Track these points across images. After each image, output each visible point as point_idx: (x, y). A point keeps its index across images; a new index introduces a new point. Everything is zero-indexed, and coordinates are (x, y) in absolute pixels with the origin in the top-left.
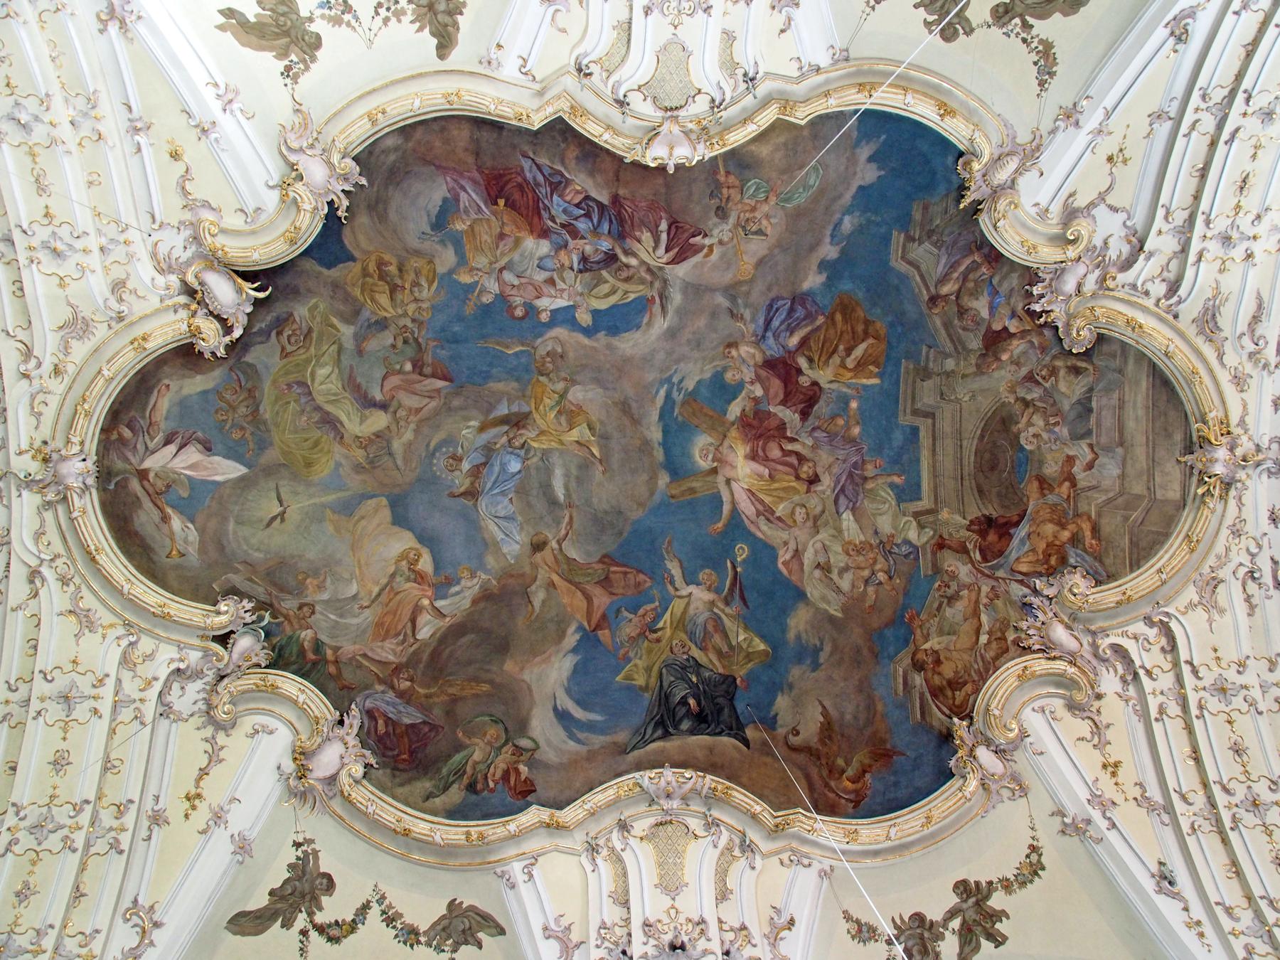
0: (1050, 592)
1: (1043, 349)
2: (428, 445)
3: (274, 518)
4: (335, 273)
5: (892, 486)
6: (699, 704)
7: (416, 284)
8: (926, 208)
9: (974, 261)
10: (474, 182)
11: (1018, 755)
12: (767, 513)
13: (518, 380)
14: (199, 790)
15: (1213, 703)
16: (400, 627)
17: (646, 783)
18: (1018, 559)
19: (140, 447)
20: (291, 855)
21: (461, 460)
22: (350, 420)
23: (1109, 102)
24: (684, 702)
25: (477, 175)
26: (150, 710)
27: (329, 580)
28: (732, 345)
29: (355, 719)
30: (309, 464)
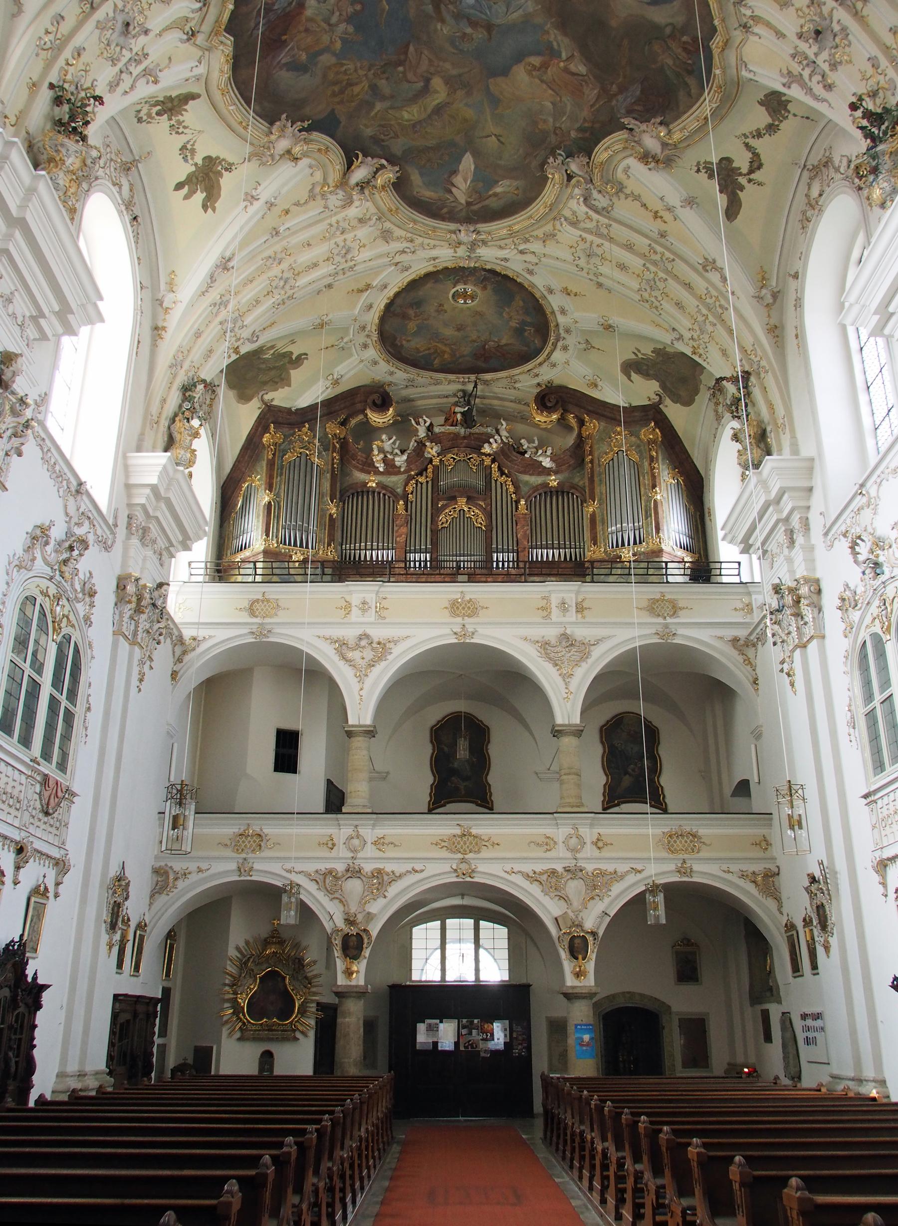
3: (499, 140)
4: (343, 119)
19: (453, 204)
20: (703, 176)
21: (465, 34)
30: (465, 120)
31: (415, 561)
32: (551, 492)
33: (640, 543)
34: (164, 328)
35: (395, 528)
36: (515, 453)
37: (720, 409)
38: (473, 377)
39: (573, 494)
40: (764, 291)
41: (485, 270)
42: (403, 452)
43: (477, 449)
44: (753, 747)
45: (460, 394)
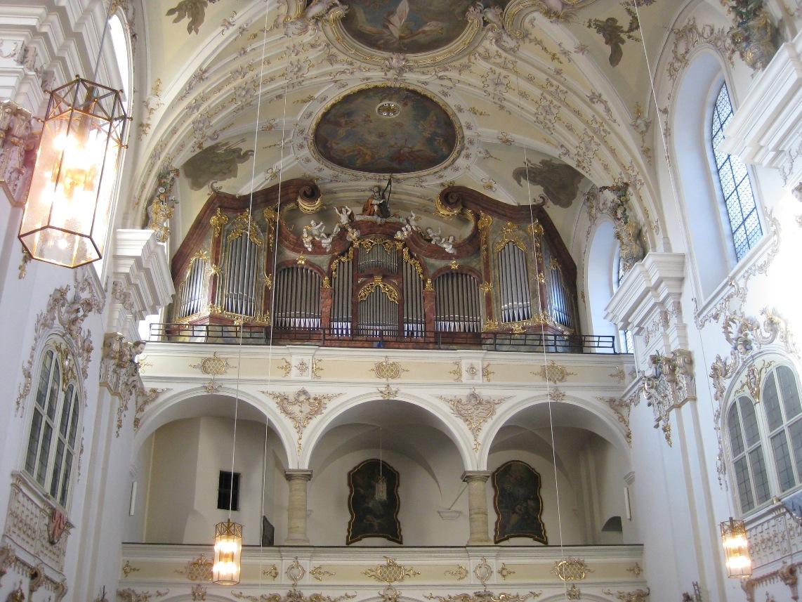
20: (593, 31)
26: (510, 57)
31: (337, 329)
32: (452, 274)
33: (528, 318)
34: (148, 125)
35: (322, 300)
36: (423, 240)
37: (594, 211)
38: (387, 176)
39: (470, 276)
40: (639, 121)
41: (408, 90)
42: (328, 235)
43: (391, 236)
44: (625, 489)
45: (376, 189)
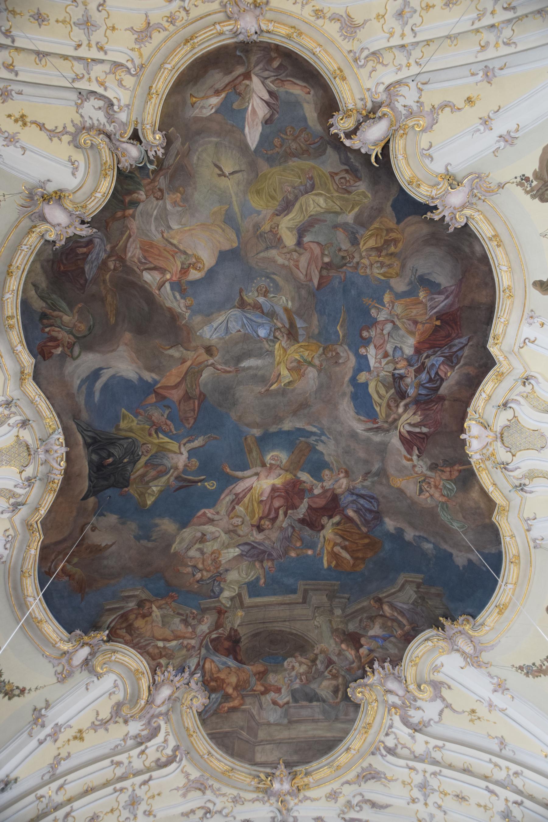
0: (193, 684)
1: (349, 670)
2: (274, 274)
3: (220, 169)
4: (389, 209)
5: (258, 579)
6: (110, 465)
7: (382, 265)
8: (438, 595)
9: (405, 626)
10: (451, 305)
11: (85, 673)
12: (238, 500)
13: (319, 333)
14: (29, 124)
15: (124, 798)
16: (150, 259)
17: (56, 436)
18: (213, 661)
19: (266, 74)
21: (265, 296)
22: (289, 220)
23: (510, 712)
24: (110, 455)
25: (456, 306)
26: (83, 85)
27: (180, 209)
28: (347, 474)
29: (85, 231)
30: (258, 192)
